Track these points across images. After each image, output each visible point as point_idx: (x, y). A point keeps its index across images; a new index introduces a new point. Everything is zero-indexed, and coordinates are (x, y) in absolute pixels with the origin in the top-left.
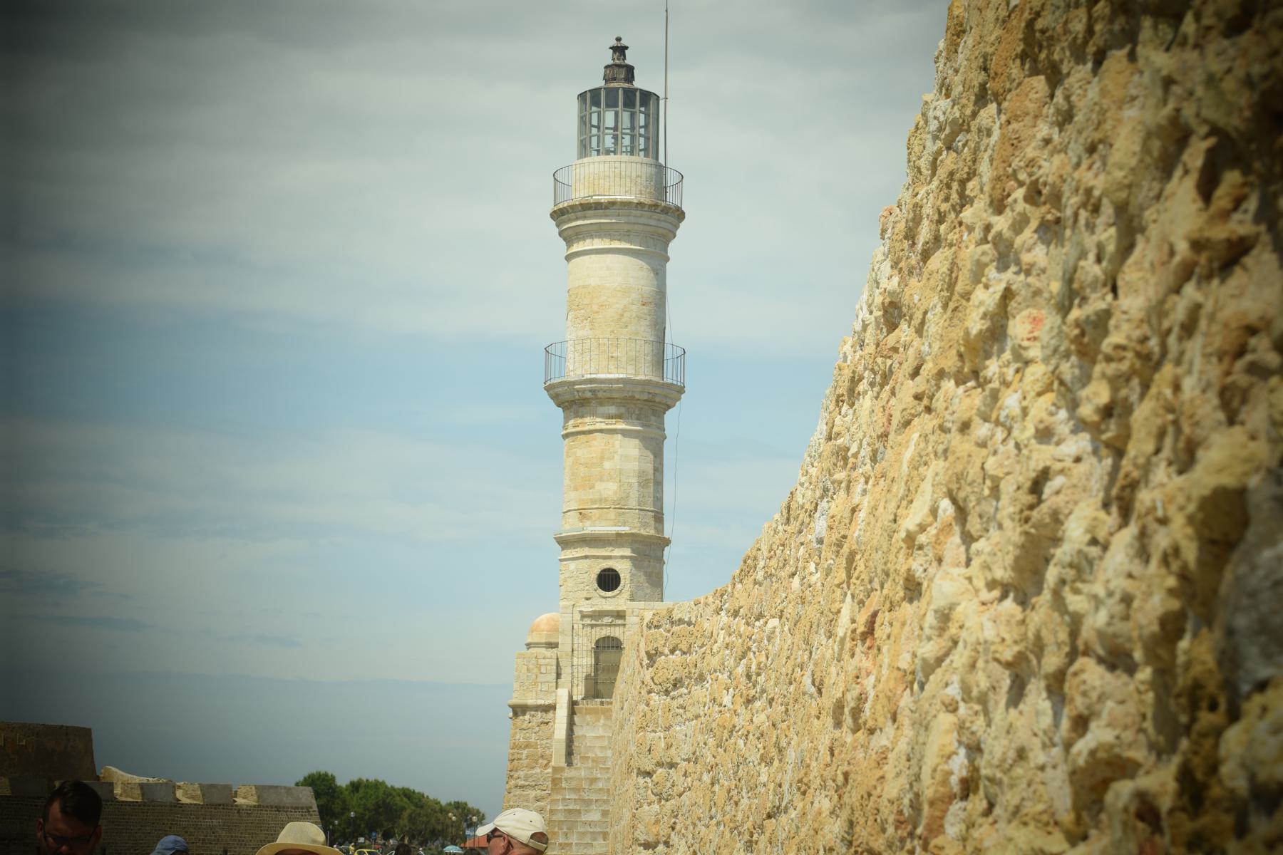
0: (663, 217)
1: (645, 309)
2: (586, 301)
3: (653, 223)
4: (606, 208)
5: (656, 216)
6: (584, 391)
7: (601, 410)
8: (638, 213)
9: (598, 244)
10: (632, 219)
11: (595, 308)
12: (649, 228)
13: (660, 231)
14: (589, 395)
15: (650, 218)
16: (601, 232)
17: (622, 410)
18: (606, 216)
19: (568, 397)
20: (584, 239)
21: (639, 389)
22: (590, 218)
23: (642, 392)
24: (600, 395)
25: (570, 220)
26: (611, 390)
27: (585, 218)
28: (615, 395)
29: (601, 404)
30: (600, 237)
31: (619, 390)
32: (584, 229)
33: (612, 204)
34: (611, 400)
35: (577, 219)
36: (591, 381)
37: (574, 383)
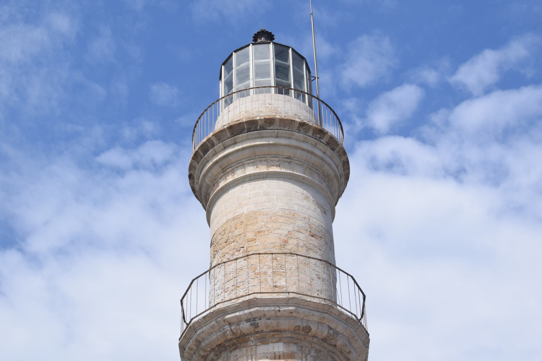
0: (329, 151)
1: (315, 242)
2: (237, 232)
3: (319, 153)
4: (262, 128)
5: (322, 146)
6: (239, 320)
7: (262, 349)
8: (301, 135)
9: (251, 170)
10: (294, 143)
11: (250, 235)
12: (313, 158)
13: (326, 167)
14: (246, 326)
15: (315, 146)
16: (255, 156)
17: (293, 348)
18: (262, 137)
19: (215, 338)
20: (233, 172)
21: (316, 317)
22: (242, 142)
23: (320, 323)
24: (262, 323)
25: (216, 154)
26: (277, 317)
27: (235, 143)
28: (284, 324)
29: (264, 341)
30: (254, 164)
31: (290, 315)
32: (232, 158)
33: (269, 122)
34: (276, 334)
35: (225, 148)
36: (250, 304)
37: (224, 312)
